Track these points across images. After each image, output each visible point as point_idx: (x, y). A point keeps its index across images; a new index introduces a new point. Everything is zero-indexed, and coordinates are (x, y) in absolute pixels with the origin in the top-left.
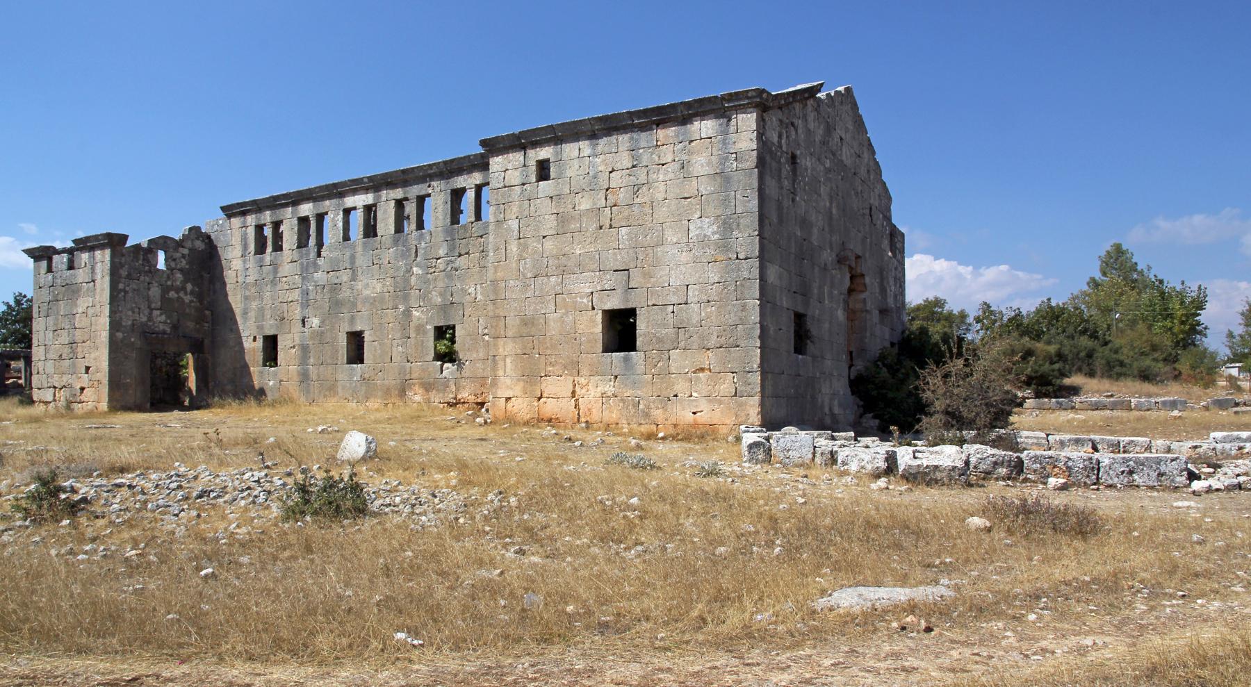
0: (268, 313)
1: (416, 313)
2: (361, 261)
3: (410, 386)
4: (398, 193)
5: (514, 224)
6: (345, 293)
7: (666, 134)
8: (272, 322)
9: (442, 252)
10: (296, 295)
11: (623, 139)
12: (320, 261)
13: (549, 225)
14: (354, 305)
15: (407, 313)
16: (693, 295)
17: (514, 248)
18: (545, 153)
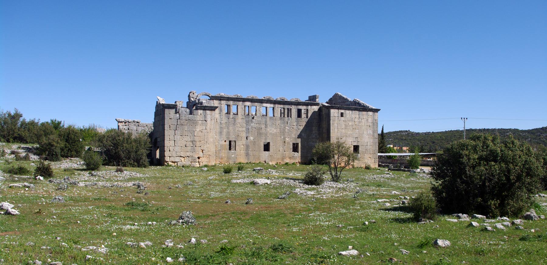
0: (231, 134)
1: (287, 139)
2: (268, 122)
3: (285, 158)
4: (282, 106)
5: (336, 125)
6: (263, 131)
7: (364, 113)
8: (234, 136)
9: (294, 124)
10: (244, 129)
11: (357, 112)
12: (254, 120)
13: (343, 126)
14: (266, 135)
15: (284, 138)
16: (369, 144)
17: (336, 130)
18: (342, 111)
